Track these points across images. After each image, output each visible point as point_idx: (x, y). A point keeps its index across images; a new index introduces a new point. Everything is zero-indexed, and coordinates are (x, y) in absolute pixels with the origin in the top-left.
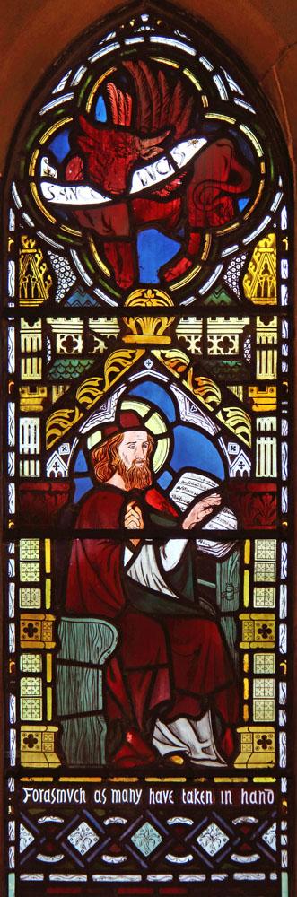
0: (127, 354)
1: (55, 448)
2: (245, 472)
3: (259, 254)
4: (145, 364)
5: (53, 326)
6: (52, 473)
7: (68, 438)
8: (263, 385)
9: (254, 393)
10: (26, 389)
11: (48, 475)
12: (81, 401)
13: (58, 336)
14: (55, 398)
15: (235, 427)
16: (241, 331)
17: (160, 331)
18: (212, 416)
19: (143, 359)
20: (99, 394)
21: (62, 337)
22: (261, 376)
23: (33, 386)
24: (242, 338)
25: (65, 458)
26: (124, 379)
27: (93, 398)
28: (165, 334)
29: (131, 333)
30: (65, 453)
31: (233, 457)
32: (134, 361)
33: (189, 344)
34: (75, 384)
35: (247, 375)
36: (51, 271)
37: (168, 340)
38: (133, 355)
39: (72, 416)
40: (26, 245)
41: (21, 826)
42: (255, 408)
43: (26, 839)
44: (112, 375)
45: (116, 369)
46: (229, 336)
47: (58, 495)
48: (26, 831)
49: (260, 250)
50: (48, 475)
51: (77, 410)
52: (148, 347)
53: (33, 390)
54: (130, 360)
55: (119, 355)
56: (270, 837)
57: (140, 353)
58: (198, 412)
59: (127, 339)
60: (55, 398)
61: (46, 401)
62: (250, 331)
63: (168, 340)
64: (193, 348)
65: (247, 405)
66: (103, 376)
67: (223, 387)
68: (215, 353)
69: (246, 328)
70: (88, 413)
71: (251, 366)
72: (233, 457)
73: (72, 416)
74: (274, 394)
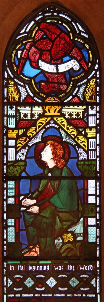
0: (44, 119)
1: (20, 150)
2: (85, 158)
3: (90, 85)
4: (51, 122)
5: (20, 110)
6: (18, 159)
7: (24, 147)
8: (91, 128)
9: (88, 131)
10: (11, 131)
11: (17, 160)
12: (29, 135)
13: (22, 113)
14: (20, 134)
15: (81, 143)
16: (83, 110)
17: (57, 112)
18: (74, 139)
19: (50, 120)
20: (35, 133)
21: (23, 113)
22: (90, 125)
23: (13, 129)
24: (83, 113)
25: (23, 154)
26: (44, 127)
27: (33, 134)
28: (58, 112)
29: (47, 113)
30: (23, 152)
31: (81, 153)
32: (47, 121)
33: (65, 115)
34: (27, 129)
35: (86, 126)
36: (19, 93)
37: (59, 114)
38: (47, 120)
39: (26, 140)
40: (11, 84)
41: (8, 279)
42: (88, 136)
43: (10, 283)
44: (39, 127)
45: (41, 124)
46: (79, 112)
47: (21, 167)
48: (9, 280)
49: (90, 84)
50: (17, 160)
51: (27, 138)
52: (52, 117)
53: (13, 131)
54: (45, 121)
55: (42, 120)
56: (93, 282)
57: (49, 119)
58: (69, 138)
59: (46, 114)
60: (20, 134)
61: (17, 134)
62: (86, 110)
63: (59, 114)
64: (67, 116)
65: (86, 135)
66: (36, 127)
67: (78, 130)
68: (74, 118)
69: (85, 109)
70: (30, 139)
71: (87, 123)
72: (81, 153)
73: (26, 140)
74: (95, 131)
